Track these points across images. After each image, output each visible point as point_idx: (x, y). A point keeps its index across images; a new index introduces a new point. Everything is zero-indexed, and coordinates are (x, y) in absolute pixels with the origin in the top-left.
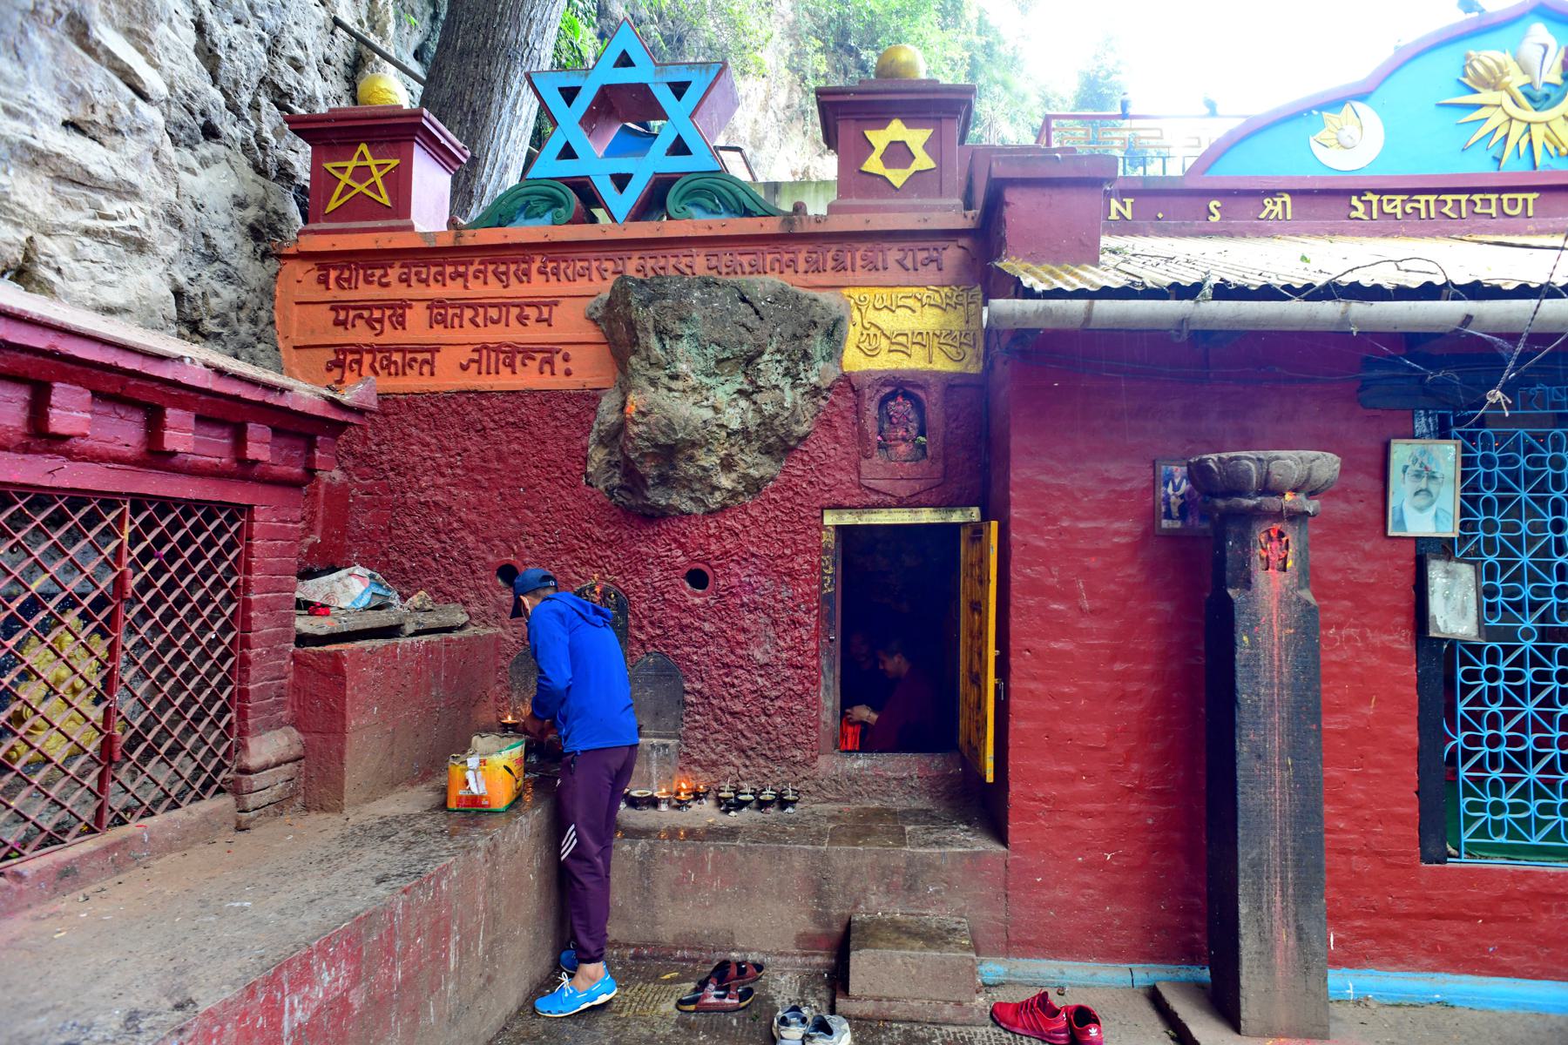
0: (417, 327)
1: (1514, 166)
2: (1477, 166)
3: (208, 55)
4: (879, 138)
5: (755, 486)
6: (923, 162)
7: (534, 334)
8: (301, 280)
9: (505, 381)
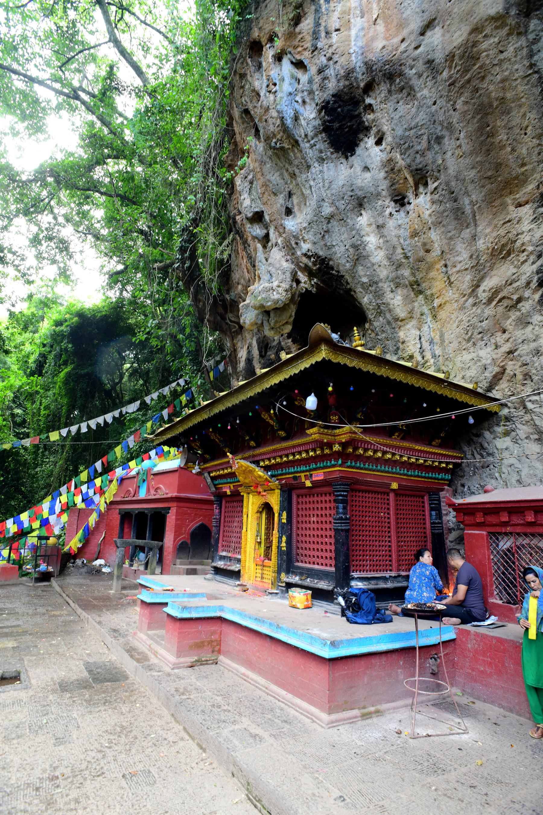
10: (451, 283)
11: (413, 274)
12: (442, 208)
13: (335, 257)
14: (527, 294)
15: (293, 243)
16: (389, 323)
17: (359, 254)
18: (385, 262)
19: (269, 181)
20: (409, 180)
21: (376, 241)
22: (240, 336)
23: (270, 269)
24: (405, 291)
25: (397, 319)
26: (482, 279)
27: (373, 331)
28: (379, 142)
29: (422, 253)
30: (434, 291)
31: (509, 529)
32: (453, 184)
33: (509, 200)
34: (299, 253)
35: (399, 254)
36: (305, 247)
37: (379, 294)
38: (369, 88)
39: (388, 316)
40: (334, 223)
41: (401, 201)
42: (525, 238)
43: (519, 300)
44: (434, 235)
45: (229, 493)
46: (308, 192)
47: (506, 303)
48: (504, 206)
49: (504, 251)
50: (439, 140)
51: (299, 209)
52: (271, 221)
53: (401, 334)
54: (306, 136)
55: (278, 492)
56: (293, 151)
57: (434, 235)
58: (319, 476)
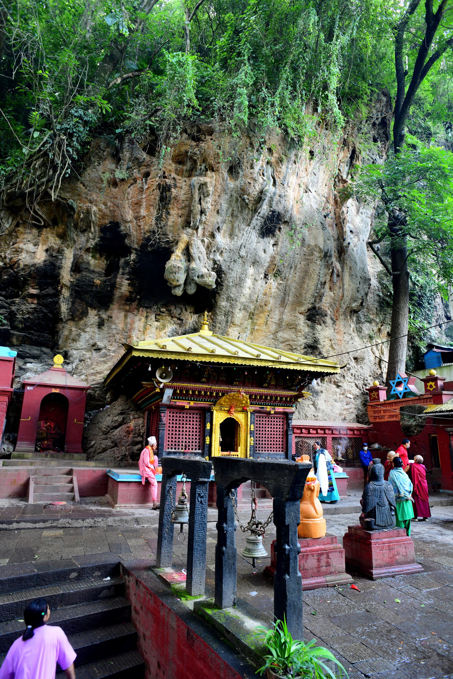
0: (382, 413)
3: (357, 386)
4: (429, 384)
5: (420, 431)
6: (434, 387)
7: (394, 414)
8: (369, 409)
9: (392, 420)
12: (279, 293)
13: (228, 275)
14: (299, 348)
16: (227, 322)
17: (240, 283)
18: (248, 296)
19: (221, 204)
20: (274, 271)
22: (35, 231)
23: (200, 255)
24: (246, 314)
25: (232, 323)
27: (212, 319)
28: (274, 245)
29: (263, 304)
30: (258, 322)
31: (301, 435)
33: (297, 308)
34: (211, 256)
35: (254, 297)
36: (218, 257)
37: (232, 306)
38: (286, 222)
39: (230, 319)
40: (240, 261)
41: (266, 276)
42: (302, 328)
43: (295, 349)
44: (272, 301)
45: (187, 407)
46: (240, 235)
47: (289, 347)
48: (295, 310)
49: (292, 326)
50: (291, 268)
53: (230, 330)
55: (249, 413)
57: (272, 301)
58: (280, 409)
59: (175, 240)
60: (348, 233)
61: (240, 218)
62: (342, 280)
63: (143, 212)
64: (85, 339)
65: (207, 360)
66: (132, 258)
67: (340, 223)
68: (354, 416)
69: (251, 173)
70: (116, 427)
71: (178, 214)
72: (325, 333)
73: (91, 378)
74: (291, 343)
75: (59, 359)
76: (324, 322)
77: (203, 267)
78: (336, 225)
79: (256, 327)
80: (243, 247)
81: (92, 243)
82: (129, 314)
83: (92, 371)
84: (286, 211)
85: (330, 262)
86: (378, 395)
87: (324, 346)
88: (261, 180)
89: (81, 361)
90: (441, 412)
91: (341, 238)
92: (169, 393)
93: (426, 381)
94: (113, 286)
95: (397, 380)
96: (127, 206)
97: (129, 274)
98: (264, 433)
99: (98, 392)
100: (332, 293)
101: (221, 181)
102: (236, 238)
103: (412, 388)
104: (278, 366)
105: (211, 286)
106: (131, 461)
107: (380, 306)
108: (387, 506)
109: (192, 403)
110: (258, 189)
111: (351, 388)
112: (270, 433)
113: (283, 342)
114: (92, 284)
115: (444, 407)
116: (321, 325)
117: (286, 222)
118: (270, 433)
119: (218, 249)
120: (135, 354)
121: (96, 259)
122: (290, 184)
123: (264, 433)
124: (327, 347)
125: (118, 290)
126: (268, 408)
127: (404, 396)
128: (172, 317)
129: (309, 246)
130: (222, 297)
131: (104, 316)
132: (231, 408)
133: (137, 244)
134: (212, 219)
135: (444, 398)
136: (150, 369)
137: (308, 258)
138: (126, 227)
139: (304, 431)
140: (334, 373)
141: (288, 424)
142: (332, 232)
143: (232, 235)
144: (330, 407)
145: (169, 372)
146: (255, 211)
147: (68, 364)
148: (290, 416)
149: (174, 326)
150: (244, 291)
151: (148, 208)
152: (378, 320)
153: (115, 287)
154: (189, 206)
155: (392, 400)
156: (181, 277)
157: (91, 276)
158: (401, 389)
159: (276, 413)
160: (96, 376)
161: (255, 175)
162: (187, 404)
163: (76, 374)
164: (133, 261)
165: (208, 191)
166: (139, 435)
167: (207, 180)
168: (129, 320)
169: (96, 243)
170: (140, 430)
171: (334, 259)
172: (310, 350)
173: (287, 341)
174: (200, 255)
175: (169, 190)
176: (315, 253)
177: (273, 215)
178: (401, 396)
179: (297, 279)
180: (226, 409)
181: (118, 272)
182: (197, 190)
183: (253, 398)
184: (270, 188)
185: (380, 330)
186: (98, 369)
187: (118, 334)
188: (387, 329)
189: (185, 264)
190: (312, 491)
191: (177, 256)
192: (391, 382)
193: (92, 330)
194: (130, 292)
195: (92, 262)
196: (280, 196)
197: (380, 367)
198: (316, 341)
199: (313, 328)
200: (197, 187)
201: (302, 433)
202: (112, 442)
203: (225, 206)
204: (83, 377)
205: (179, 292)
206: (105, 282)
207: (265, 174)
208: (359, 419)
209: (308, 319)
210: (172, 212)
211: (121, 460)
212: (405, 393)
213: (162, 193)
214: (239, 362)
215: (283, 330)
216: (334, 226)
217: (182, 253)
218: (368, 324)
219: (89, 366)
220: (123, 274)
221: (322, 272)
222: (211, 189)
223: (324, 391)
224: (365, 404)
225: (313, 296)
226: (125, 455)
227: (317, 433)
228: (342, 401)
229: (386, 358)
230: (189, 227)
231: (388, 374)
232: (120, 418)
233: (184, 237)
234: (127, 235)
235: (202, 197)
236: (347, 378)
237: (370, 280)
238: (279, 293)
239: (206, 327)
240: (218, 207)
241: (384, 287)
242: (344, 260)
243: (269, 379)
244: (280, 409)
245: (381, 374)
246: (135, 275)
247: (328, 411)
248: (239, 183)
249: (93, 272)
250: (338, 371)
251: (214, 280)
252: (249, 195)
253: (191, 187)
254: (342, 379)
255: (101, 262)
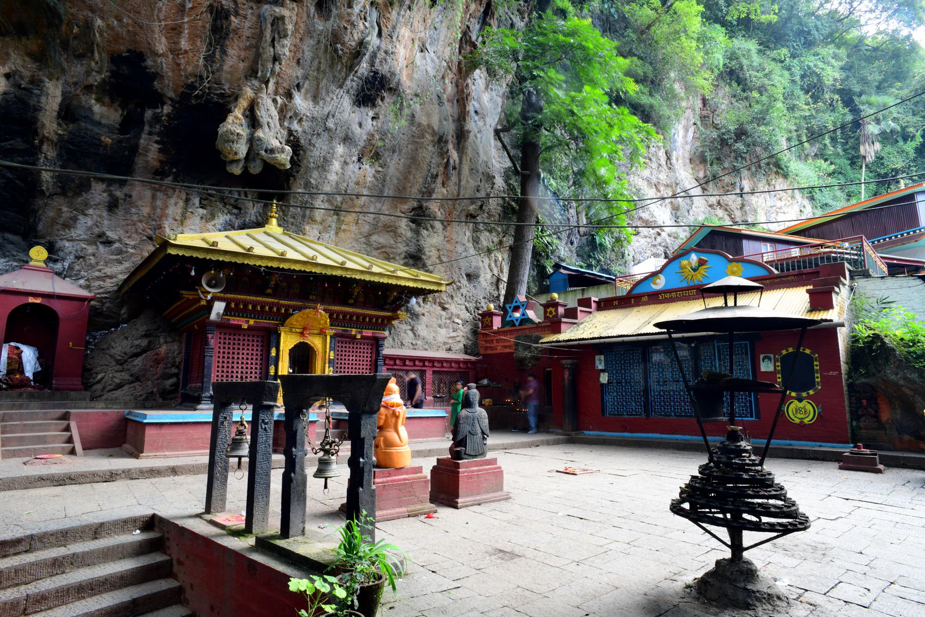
0: (495, 344)
1: (691, 284)
2: (684, 285)
3: (467, 310)
4: (548, 310)
10: (357, 223)
11: (342, 203)
12: (376, 183)
13: (308, 153)
14: (397, 258)
15: (289, 114)
17: (324, 166)
18: (334, 184)
19: (303, 51)
20: (372, 153)
21: (341, 168)
23: (270, 120)
26: (374, 233)
27: (283, 211)
28: (373, 118)
30: (346, 219)
32: (388, 178)
34: (286, 124)
35: (343, 186)
36: (295, 126)
43: (393, 258)
47: (385, 255)
49: (391, 229)
50: (394, 151)
51: (305, 94)
52: (279, 74)
54: (356, 72)
55: (328, 338)
56: (342, 68)
58: (368, 333)
59: (233, 93)
60: (472, 113)
61: (329, 75)
62: (459, 174)
63: (184, 44)
64: (84, 225)
65: (275, 265)
66: (165, 111)
67: (462, 98)
68: (461, 346)
69: (349, 14)
70: (137, 355)
71: (239, 56)
72: (432, 241)
73: (97, 283)
74: (388, 250)
75: (38, 254)
76: (432, 227)
77: (272, 136)
78: (458, 101)
79: (343, 227)
80: (331, 116)
81: (96, 79)
82: (159, 194)
83: (97, 274)
84: (393, 74)
85: (445, 150)
86: (492, 322)
87: (430, 257)
88: (361, 27)
89: (78, 258)
90: (557, 342)
91: (461, 118)
92: (219, 307)
93: (546, 306)
94: (134, 150)
95: (514, 304)
96: (157, 30)
97: (159, 134)
98: (347, 362)
99: (107, 305)
100: (444, 191)
101: (305, 18)
102: (321, 103)
103: (531, 314)
104: (367, 278)
105: (284, 165)
106: (160, 400)
107: (504, 212)
108: (480, 435)
109: (252, 322)
110: (356, 38)
111: (461, 311)
112: (354, 362)
113: (378, 249)
114: (99, 144)
115: (562, 337)
116: (427, 230)
117: (390, 89)
118: (354, 362)
119: (296, 114)
120: (173, 252)
121: (103, 104)
122: (400, 38)
123: (347, 362)
124: (434, 259)
125: (141, 158)
126: (354, 332)
127: (520, 324)
128: (225, 204)
129: (419, 125)
130: (299, 181)
131: (118, 194)
132: (305, 329)
133: (175, 91)
134: (289, 71)
135: (563, 326)
136: (193, 273)
137: (416, 139)
138: (155, 62)
139: (398, 362)
140: (437, 291)
141: (378, 353)
142: (450, 109)
143: (316, 98)
144: (433, 334)
145: (220, 278)
146: (351, 68)
147: (56, 261)
148: (381, 342)
149: (228, 217)
150: (329, 177)
151: (192, 39)
152: (500, 230)
153: (137, 151)
154: (257, 47)
155: (507, 328)
156: (242, 149)
157: (96, 130)
158: (517, 315)
159: (363, 338)
160: (104, 281)
161: (354, 18)
162: (245, 323)
163: (70, 276)
164: (168, 115)
165: (285, 30)
166: (173, 365)
167: (286, 13)
168: (159, 203)
169: (104, 80)
170: (174, 358)
171: (450, 146)
172: (411, 262)
173: (382, 247)
174: (270, 120)
175: (227, 17)
176: (427, 136)
177: (374, 77)
178: (517, 324)
179: (401, 167)
180: (298, 330)
181: (142, 130)
182: (269, 26)
183: (335, 319)
184: (373, 40)
185: (501, 242)
186: (108, 271)
187: (141, 221)
188: (509, 241)
189: (248, 131)
190: (397, 417)
191: (236, 117)
192: (507, 306)
193: (98, 212)
194: (161, 161)
195: (97, 108)
196: (386, 52)
197: (498, 288)
198: (420, 250)
199: (417, 233)
200: (270, 20)
201: (395, 364)
202: (132, 375)
203: (308, 55)
204: (82, 282)
205: (237, 170)
206: (120, 142)
207: (368, 19)
208: (466, 350)
209: (413, 221)
210: (231, 52)
211: (146, 399)
212: (522, 320)
213: (215, 20)
214: (318, 270)
215: (378, 233)
216: (455, 102)
217: (243, 115)
218: (488, 234)
219: (92, 267)
220: (150, 133)
221: (433, 161)
222: (290, 27)
223: (426, 314)
224: (475, 332)
225: (421, 192)
226: (152, 392)
227: (415, 365)
228: (447, 327)
229: (505, 278)
230: (256, 77)
231: (506, 296)
232: (144, 343)
233: (249, 92)
234: (156, 76)
235: (276, 36)
236: (455, 299)
237: (494, 177)
238: (376, 183)
239: (274, 221)
240: (299, 55)
241: (511, 188)
242: (463, 148)
243: (356, 293)
244: (368, 333)
245: (498, 297)
246: (170, 138)
247: (430, 338)
248: (331, 24)
249: (99, 124)
250: (443, 288)
251: (289, 158)
252: (343, 44)
253: (260, 18)
254: (450, 301)
255: (112, 111)
